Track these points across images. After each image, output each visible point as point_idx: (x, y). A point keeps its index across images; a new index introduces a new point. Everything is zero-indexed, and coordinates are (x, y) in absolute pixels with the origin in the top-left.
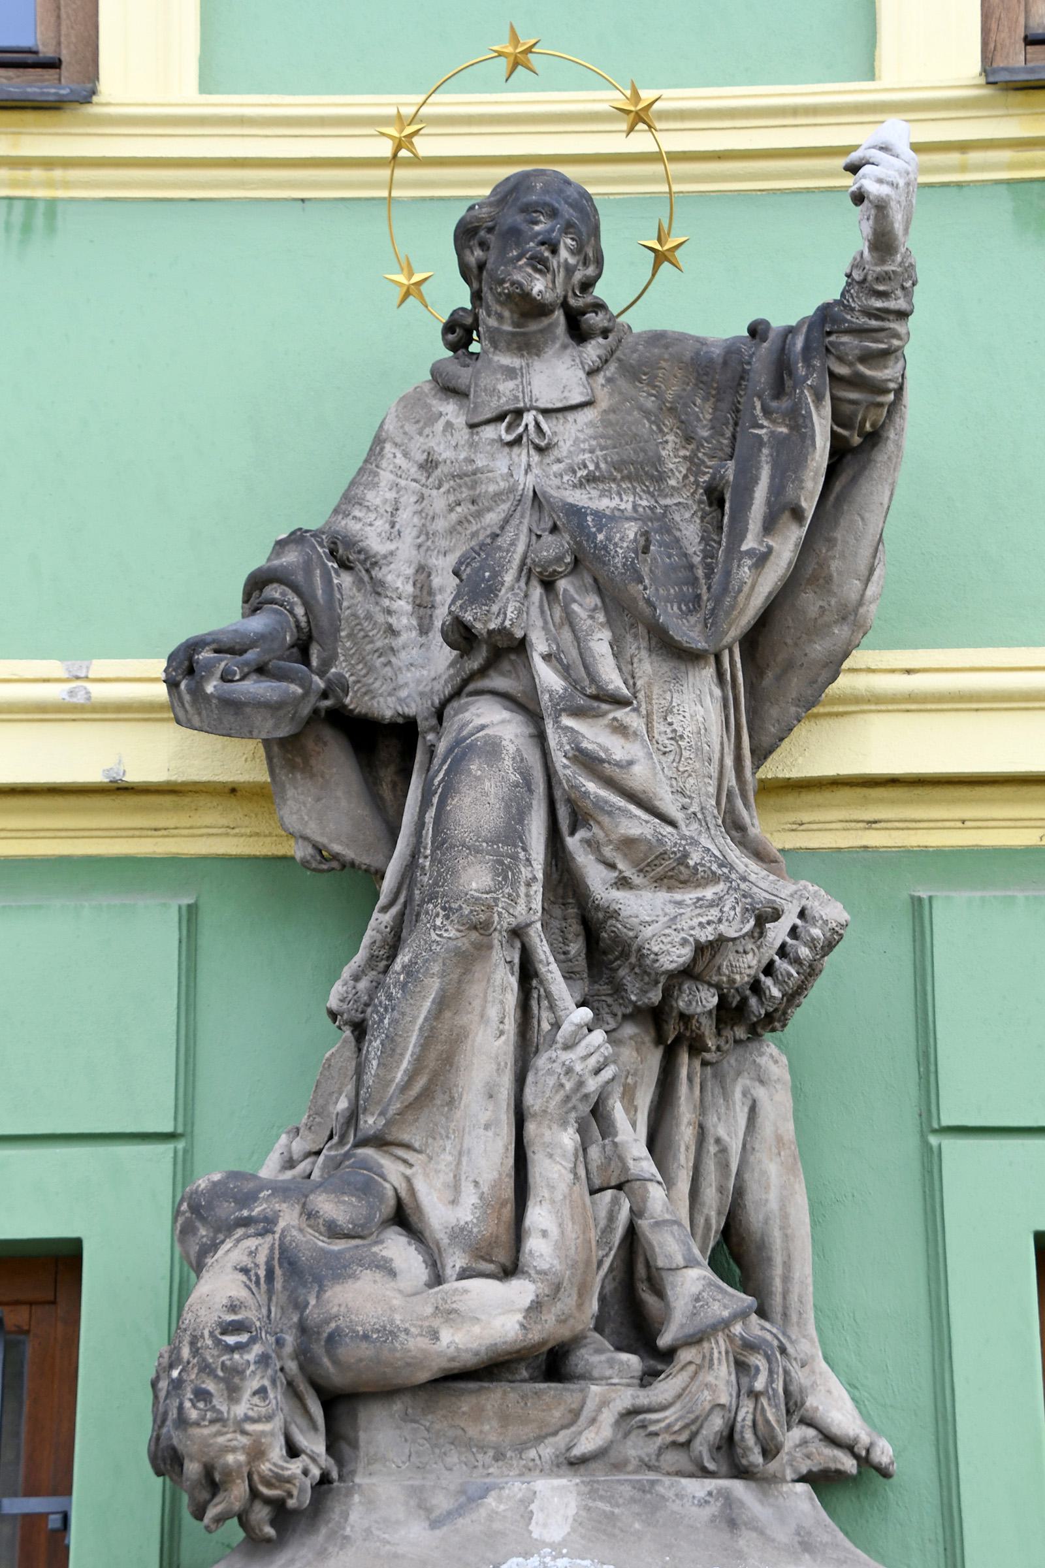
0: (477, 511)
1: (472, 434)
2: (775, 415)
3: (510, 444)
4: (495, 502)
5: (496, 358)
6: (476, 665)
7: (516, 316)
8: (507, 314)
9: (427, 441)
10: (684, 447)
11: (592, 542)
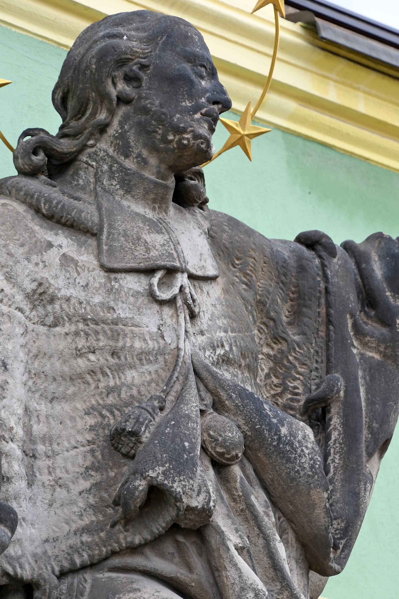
0: (116, 364)
1: (110, 280)
2: (368, 338)
3: (162, 303)
4: (141, 360)
5: (125, 203)
6: (137, 540)
7: (163, 167)
8: (153, 161)
9: (36, 269)
10: (268, 345)
11: (275, 435)
